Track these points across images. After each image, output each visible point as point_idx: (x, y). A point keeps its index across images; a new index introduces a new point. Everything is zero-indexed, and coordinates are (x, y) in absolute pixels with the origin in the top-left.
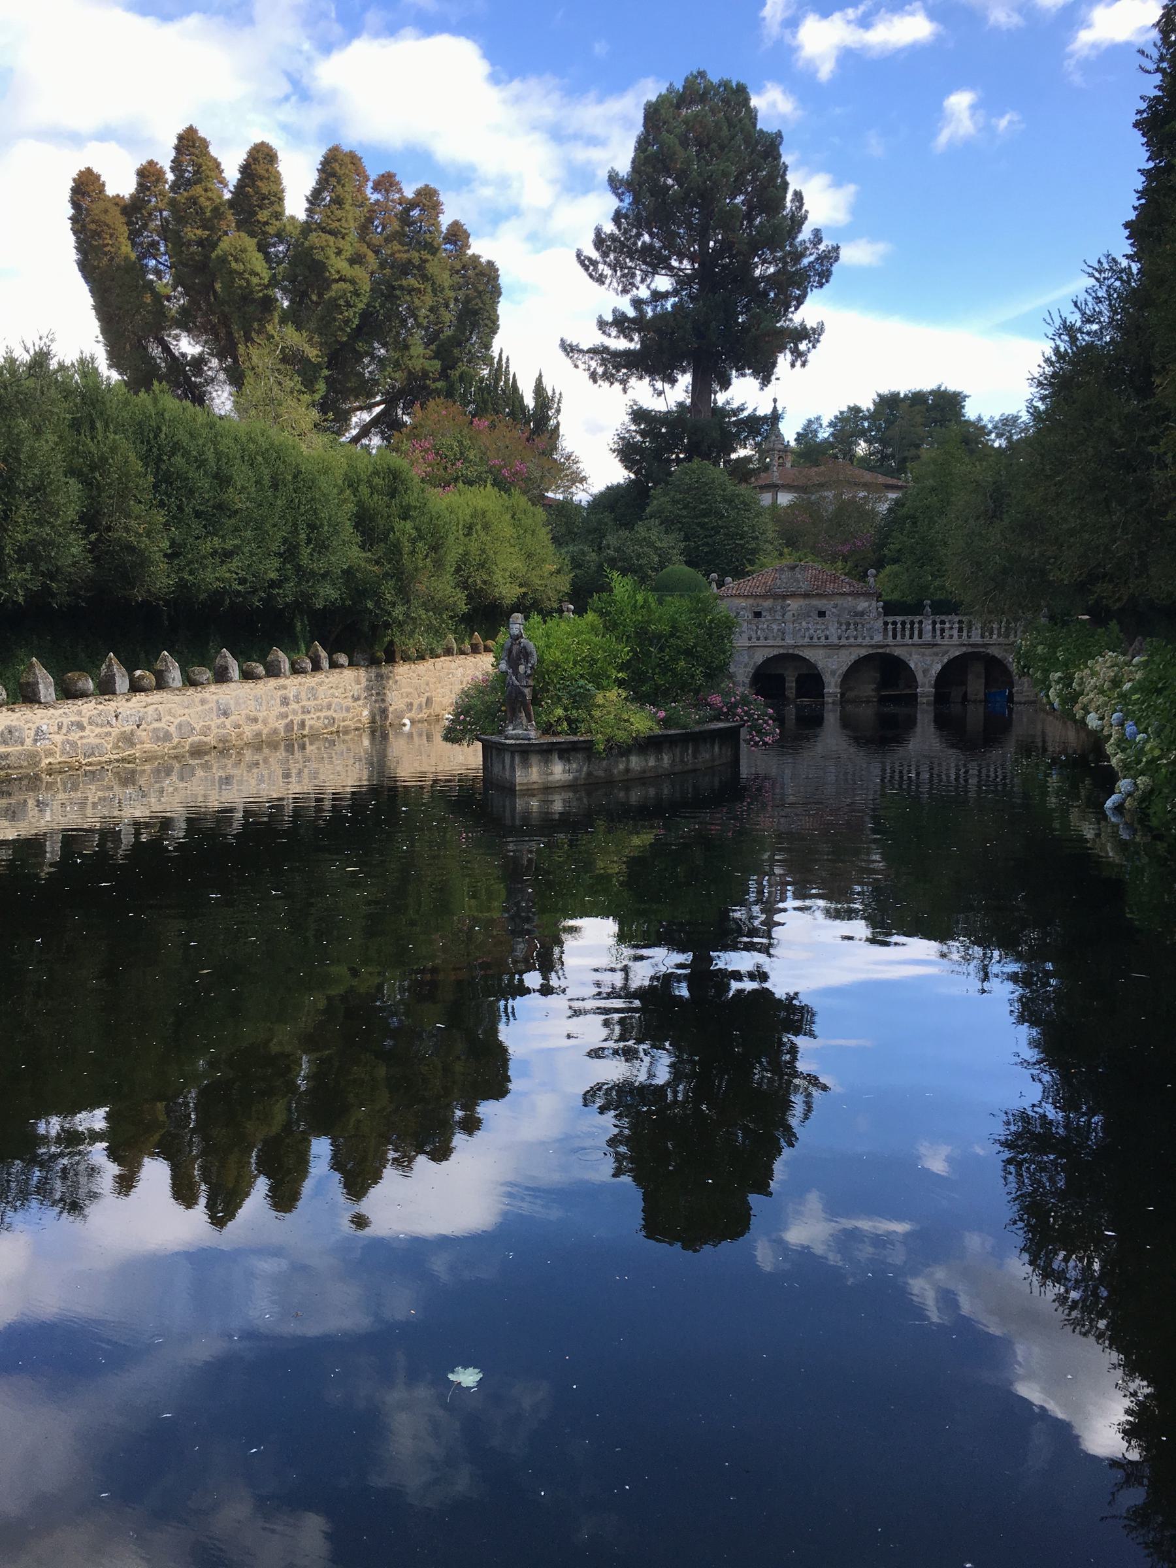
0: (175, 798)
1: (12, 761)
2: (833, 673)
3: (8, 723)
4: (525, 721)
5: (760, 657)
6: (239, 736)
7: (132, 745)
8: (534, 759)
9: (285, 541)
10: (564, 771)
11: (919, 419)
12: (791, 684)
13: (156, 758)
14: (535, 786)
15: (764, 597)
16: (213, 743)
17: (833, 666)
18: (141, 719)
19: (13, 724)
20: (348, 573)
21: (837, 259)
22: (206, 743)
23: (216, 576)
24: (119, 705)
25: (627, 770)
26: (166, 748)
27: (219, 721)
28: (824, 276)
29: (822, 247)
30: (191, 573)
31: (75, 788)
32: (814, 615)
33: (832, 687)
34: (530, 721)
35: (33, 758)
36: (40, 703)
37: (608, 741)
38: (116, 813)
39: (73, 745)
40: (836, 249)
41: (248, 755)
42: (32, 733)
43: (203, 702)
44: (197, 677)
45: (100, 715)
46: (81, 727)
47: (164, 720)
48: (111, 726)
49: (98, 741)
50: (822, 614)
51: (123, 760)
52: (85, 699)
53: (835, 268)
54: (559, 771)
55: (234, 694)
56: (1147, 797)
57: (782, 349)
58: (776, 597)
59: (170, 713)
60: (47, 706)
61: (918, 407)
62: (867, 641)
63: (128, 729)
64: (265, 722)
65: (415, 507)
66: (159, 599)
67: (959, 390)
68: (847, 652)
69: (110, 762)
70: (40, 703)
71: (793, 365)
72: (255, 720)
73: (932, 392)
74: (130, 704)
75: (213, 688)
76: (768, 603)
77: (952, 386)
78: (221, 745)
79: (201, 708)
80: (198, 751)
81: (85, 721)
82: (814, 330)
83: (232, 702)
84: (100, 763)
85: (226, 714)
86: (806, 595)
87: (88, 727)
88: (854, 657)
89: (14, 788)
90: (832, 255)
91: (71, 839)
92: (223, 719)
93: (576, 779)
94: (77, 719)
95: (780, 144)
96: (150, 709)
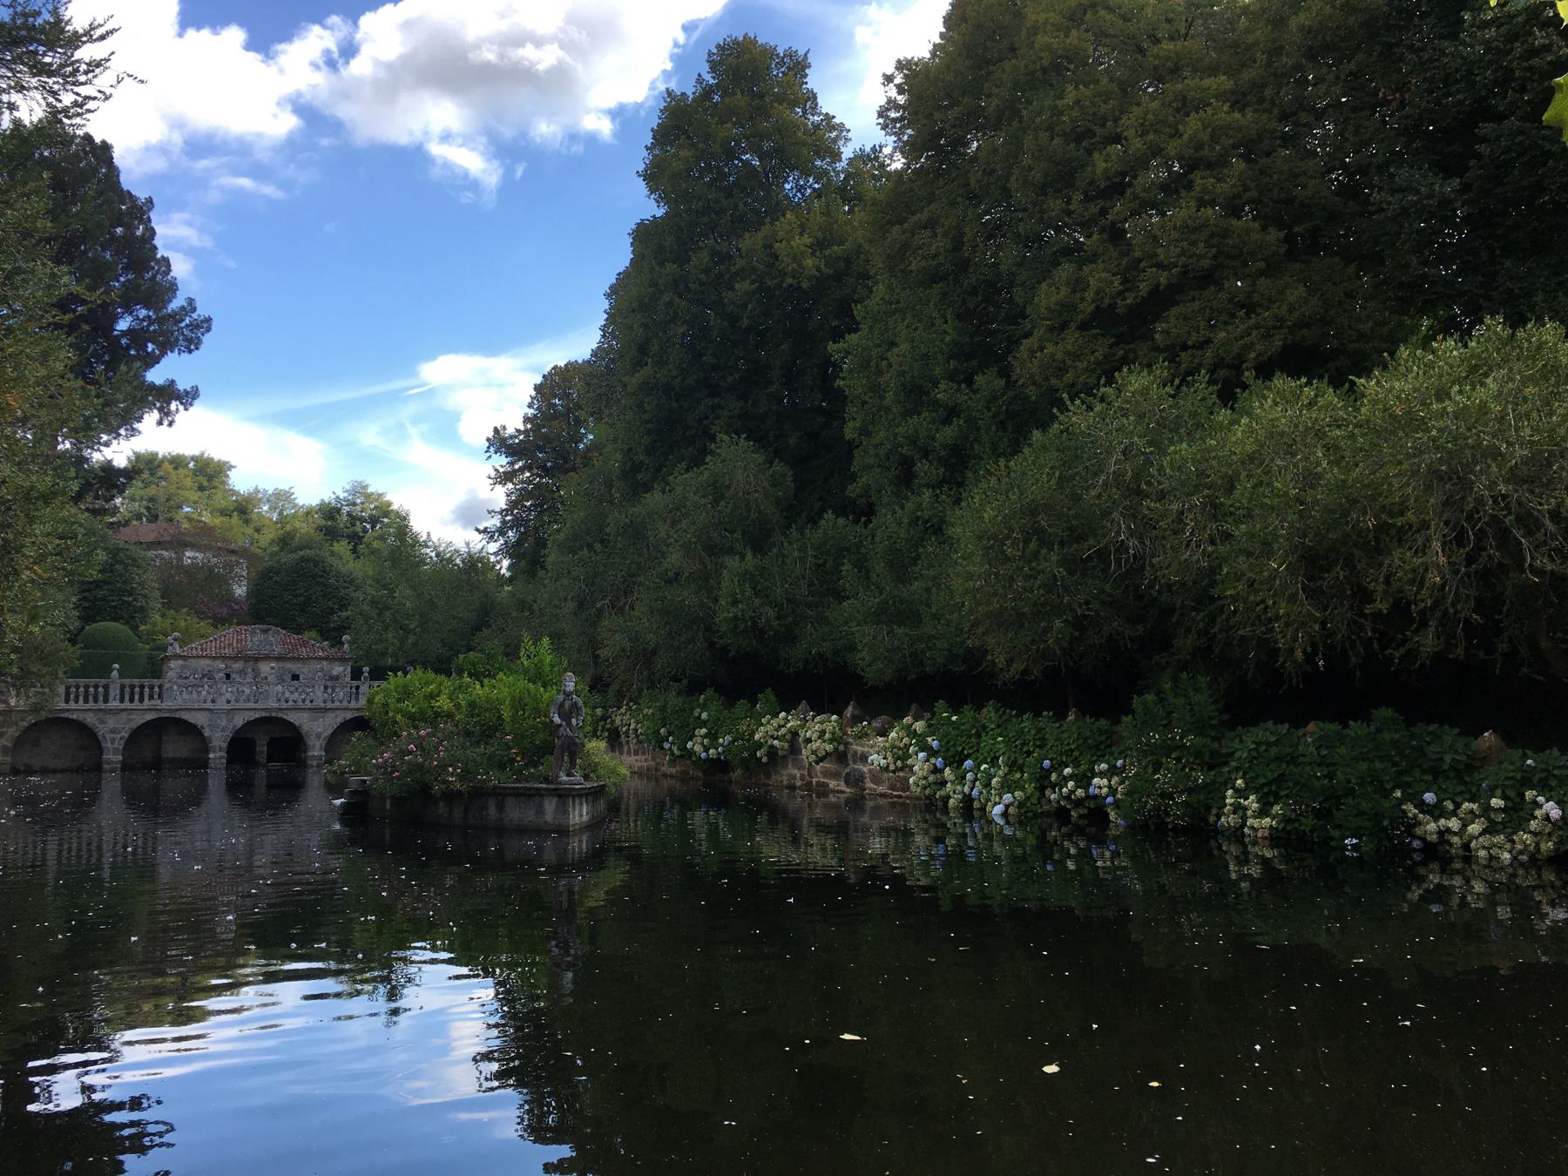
2: (318, 736)
5: (239, 721)
11: (189, 482)
12: (262, 748)
15: (235, 659)
17: (317, 729)
21: (209, 330)
28: (192, 344)
29: (195, 316)
32: (288, 677)
33: (316, 750)
40: (209, 320)
50: (295, 677)
53: (206, 339)
56: (1021, 805)
57: (151, 406)
58: (247, 659)
61: (181, 471)
62: (353, 704)
67: (224, 458)
68: (331, 715)
71: (160, 423)
73: (193, 458)
76: (238, 665)
77: (217, 453)
82: (187, 393)
86: (280, 659)
88: (340, 720)
90: (206, 324)
95: (150, 210)
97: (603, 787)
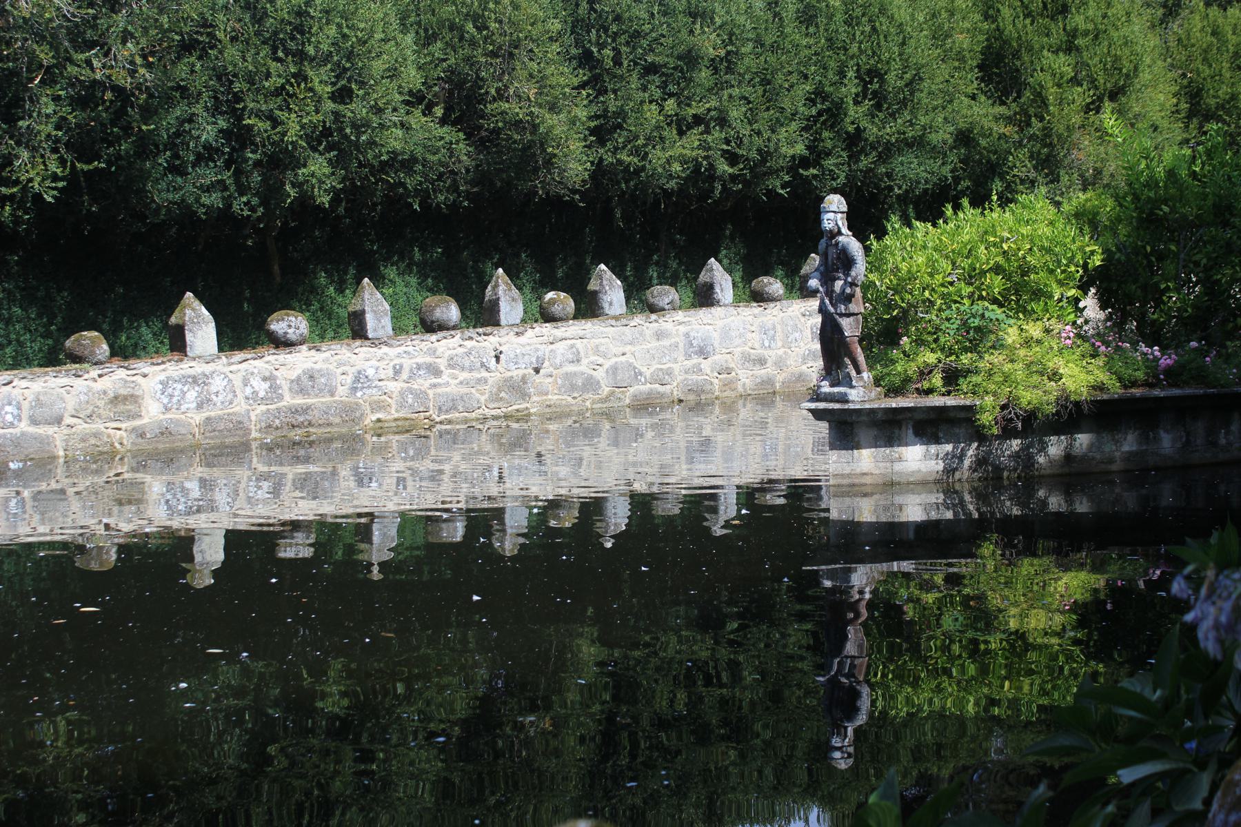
0: (613, 471)
1: (314, 416)
3: (309, 365)
4: (853, 373)
6: (727, 385)
7: (525, 396)
8: (863, 434)
9: (819, 94)
10: (926, 456)
13: (568, 415)
14: (868, 480)
16: (677, 394)
18: (541, 361)
19: (317, 367)
20: (964, 138)
22: (662, 395)
23: (671, 158)
24: (503, 340)
25: (1068, 457)
26: (589, 401)
27: (689, 363)
30: (636, 152)
31: (421, 454)
34: (859, 372)
35: (350, 412)
36: (367, 338)
37: (1004, 407)
38: (494, 491)
39: (420, 395)
41: (745, 413)
42: (349, 379)
43: (659, 335)
44: (655, 301)
45: (468, 354)
46: (437, 372)
47: (585, 361)
48: (488, 370)
49: (464, 390)
51: (507, 417)
52: (444, 333)
54: (917, 459)
55: (720, 323)
59: (596, 351)
60: (377, 343)
63: (516, 374)
64: (780, 364)
65: (1086, 33)
66: (574, 191)
69: (485, 419)
70: (367, 338)
72: (762, 362)
74: (522, 339)
75: (680, 315)
78: (692, 397)
79: (655, 344)
80: (643, 406)
81: (442, 363)
83: (715, 335)
84: (466, 421)
85: (703, 352)
87: (447, 372)
89: (315, 452)
91: (419, 524)
92: (696, 360)
93: (949, 471)
94: (428, 359)
96: (561, 347)
97: (970, 409)
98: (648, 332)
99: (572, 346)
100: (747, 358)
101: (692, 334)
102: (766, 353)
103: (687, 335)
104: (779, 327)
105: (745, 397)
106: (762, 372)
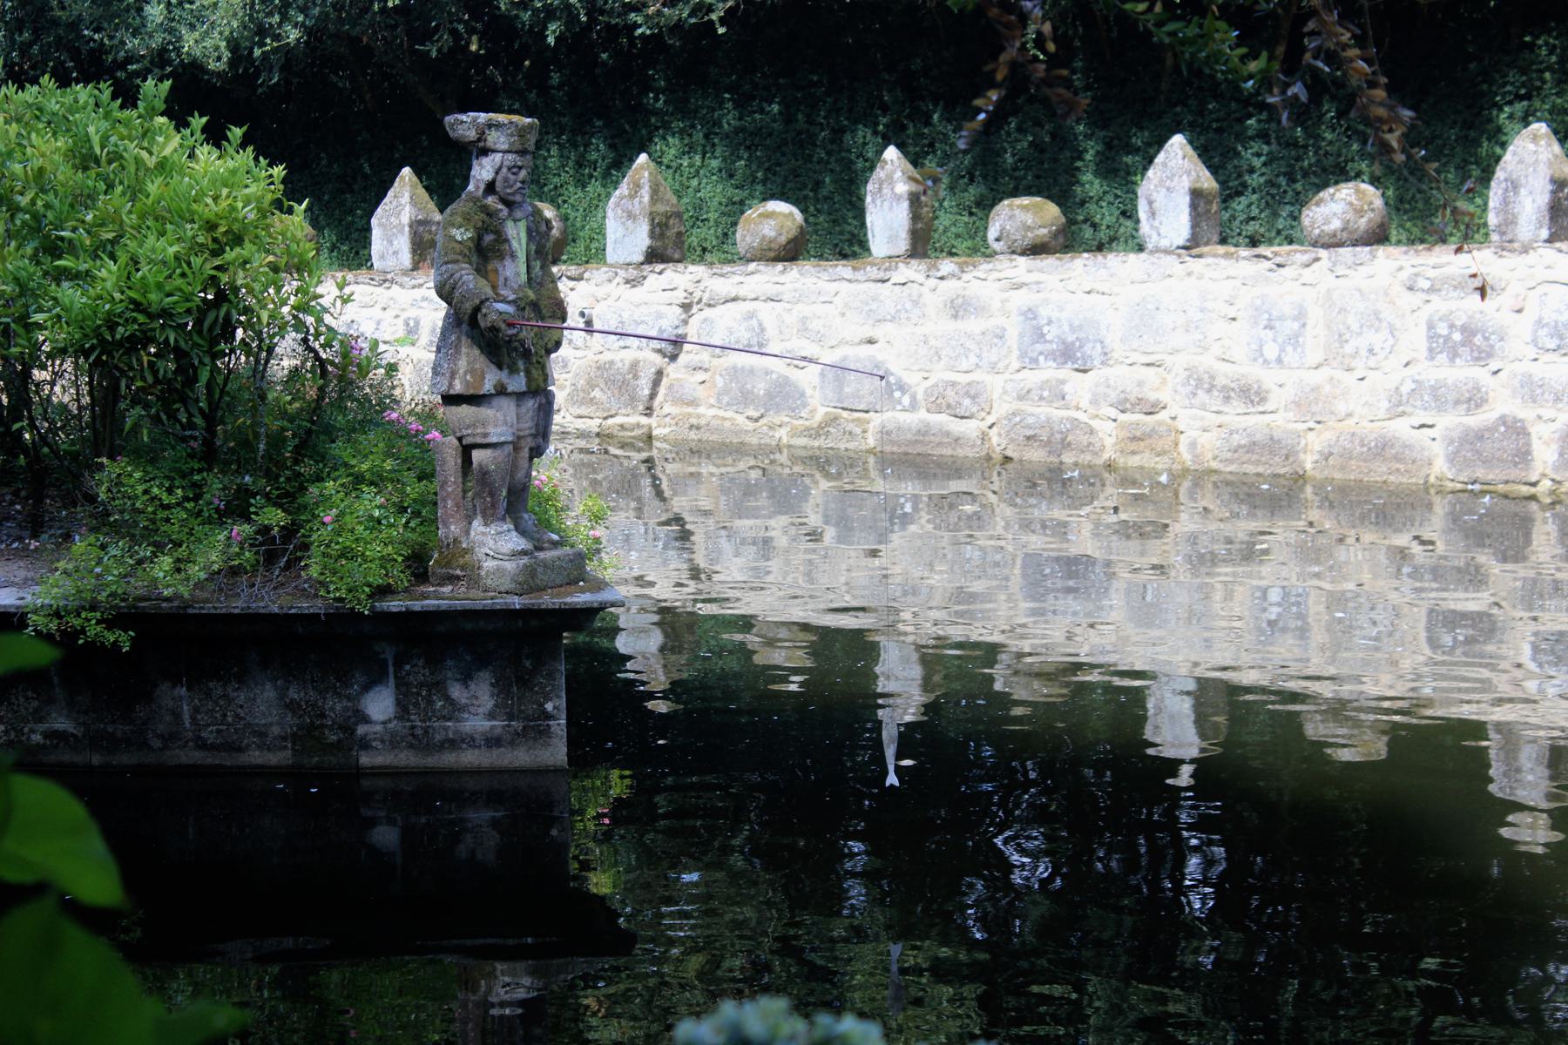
24: (601, 292)
27: (1032, 378)
43: (958, 309)
60: (385, 281)
72: (1252, 395)
79: (951, 326)
85: (1067, 354)
92: (1049, 371)
98: (928, 297)
99: (751, 316)
100: (1202, 383)
101: (1044, 312)
102: (1268, 378)
103: (1030, 314)
104: (1315, 315)
105: (1200, 477)
106: (1246, 422)
